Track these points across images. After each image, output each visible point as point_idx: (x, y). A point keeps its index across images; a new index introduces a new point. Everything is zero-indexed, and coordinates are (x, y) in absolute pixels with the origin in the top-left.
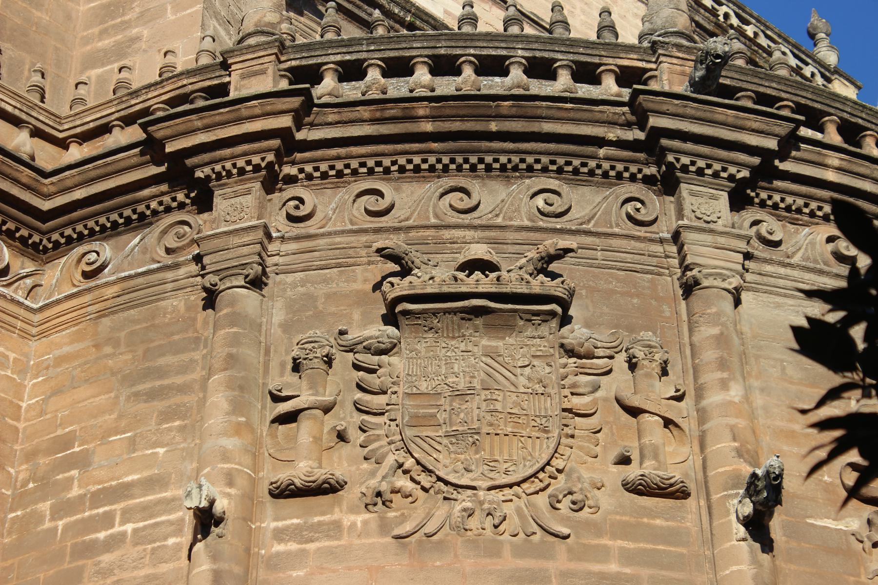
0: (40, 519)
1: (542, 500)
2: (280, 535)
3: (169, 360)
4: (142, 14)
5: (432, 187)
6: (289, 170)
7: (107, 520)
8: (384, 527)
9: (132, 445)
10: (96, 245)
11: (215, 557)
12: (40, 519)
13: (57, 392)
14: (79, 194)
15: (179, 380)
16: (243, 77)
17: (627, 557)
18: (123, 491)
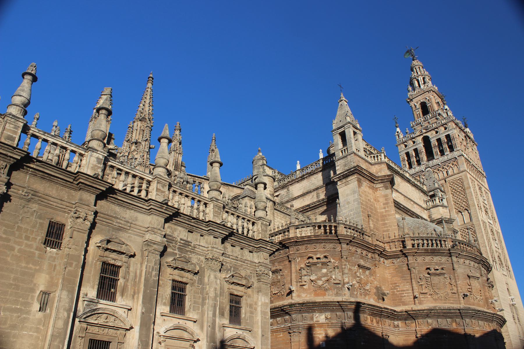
0: (395, 292)
1: (445, 295)
2: (422, 298)
3: (405, 276)
4: (389, 226)
5: (429, 257)
6: (415, 255)
7: (403, 294)
8: (432, 297)
9: (404, 285)
10: (393, 259)
11: (418, 301)
12: (395, 292)
13: (393, 277)
14: (392, 254)
15: (407, 278)
16: (407, 240)
17: (453, 300)
18: (404, 291)
